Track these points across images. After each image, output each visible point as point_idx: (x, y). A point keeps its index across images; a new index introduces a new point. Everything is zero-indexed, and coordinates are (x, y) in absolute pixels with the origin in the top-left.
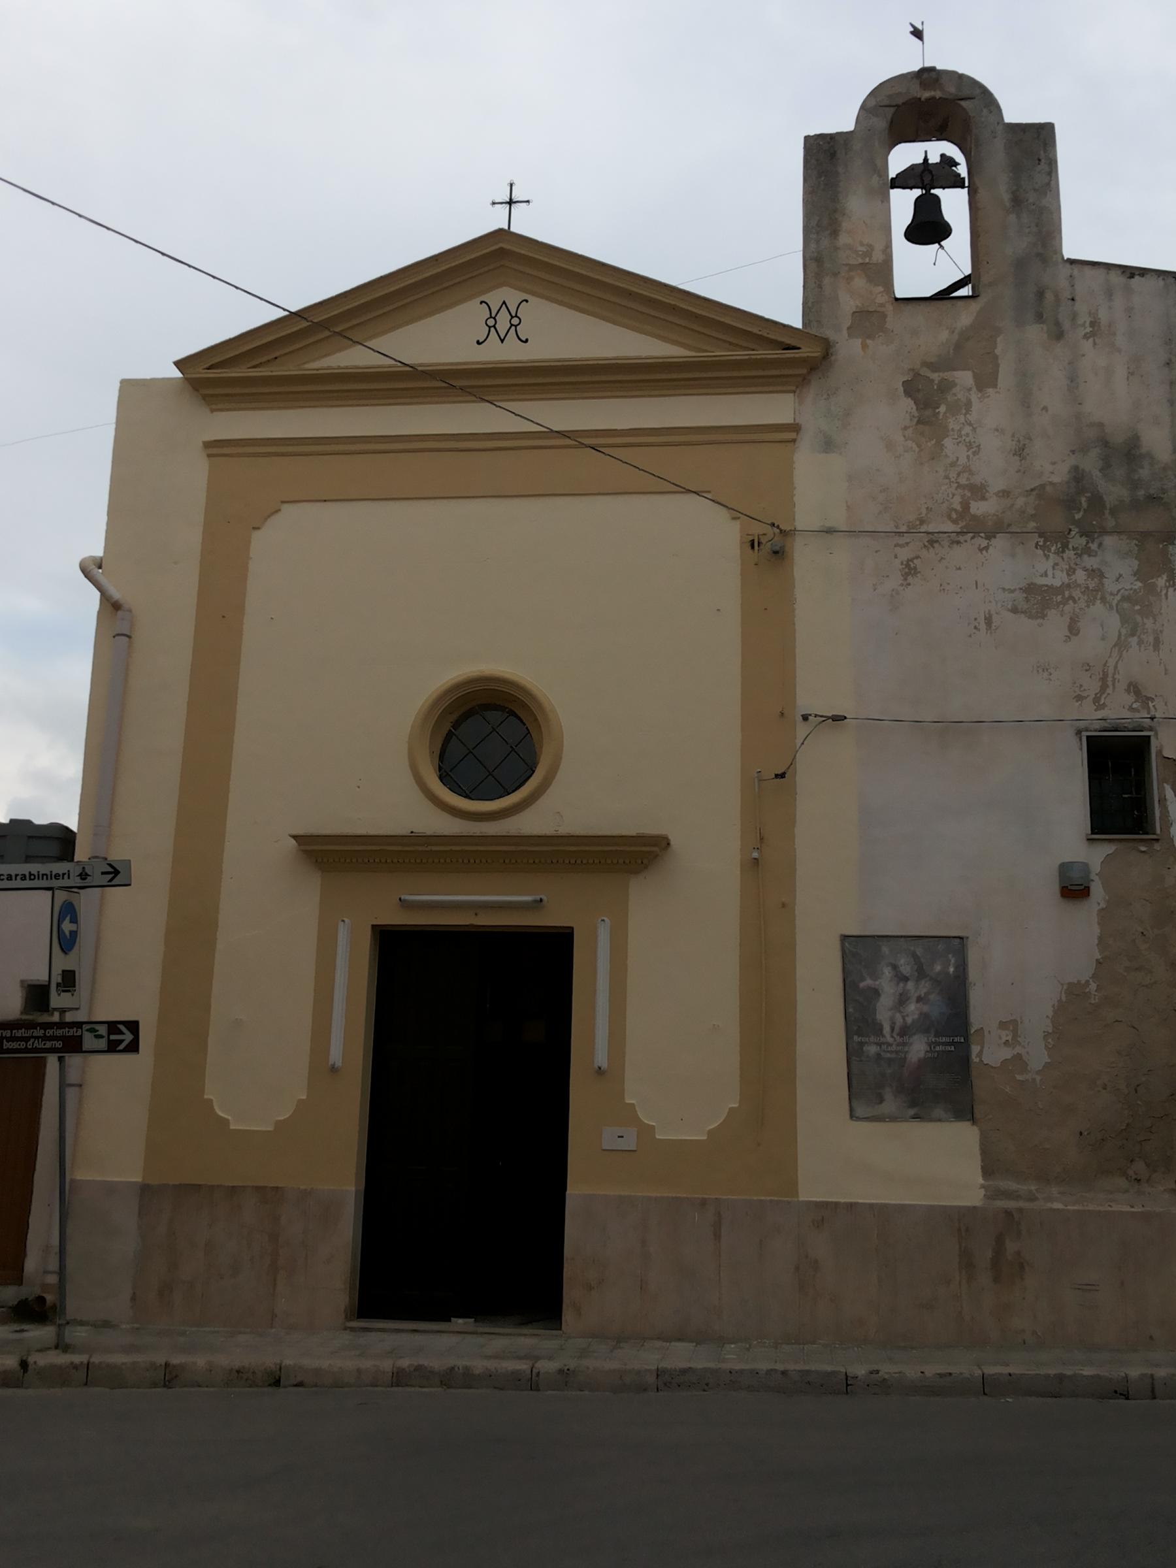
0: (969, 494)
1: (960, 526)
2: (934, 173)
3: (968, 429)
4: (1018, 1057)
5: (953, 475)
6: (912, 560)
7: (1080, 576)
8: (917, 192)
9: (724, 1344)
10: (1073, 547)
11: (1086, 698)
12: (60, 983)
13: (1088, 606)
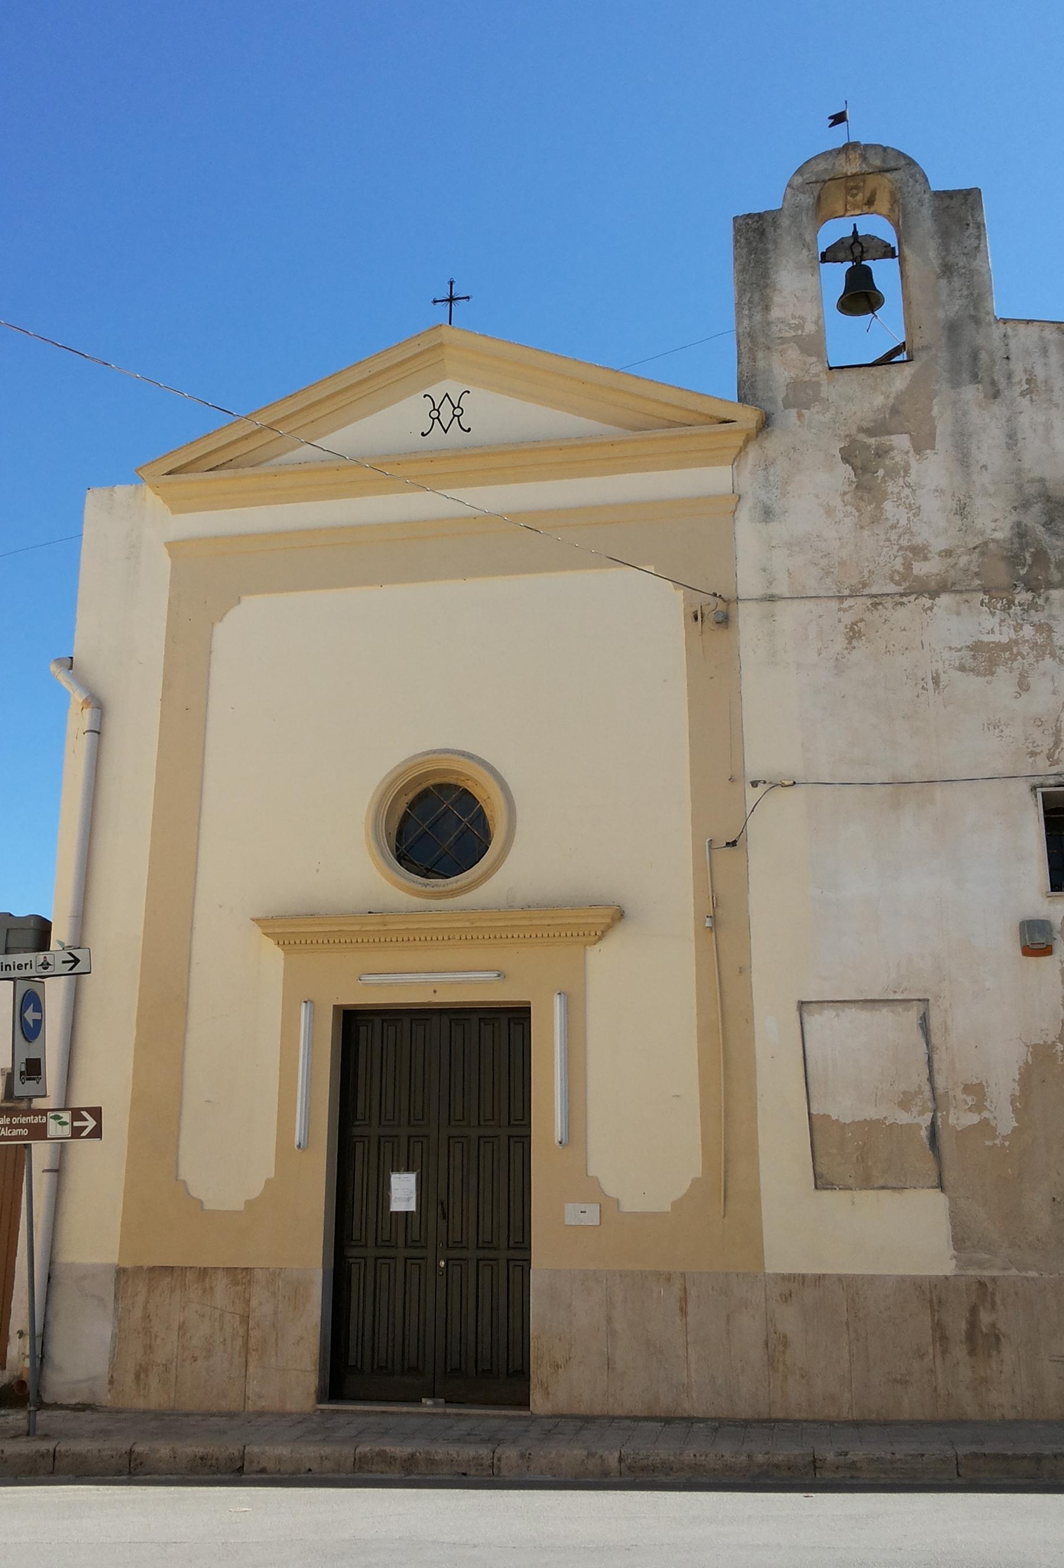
0: (911, 555)
1: (903, 587)
2: (864, 245)
3: (907, 491)
4: (985, 1122)
5: (894, 537)
6: (855, 624)
7: (1028, 631)
8: (849, 265)
9: (692, 1423)
10: (1019, 603)
11: (1039, 754)
12: (23, 1072)
13: (1037, 661)
